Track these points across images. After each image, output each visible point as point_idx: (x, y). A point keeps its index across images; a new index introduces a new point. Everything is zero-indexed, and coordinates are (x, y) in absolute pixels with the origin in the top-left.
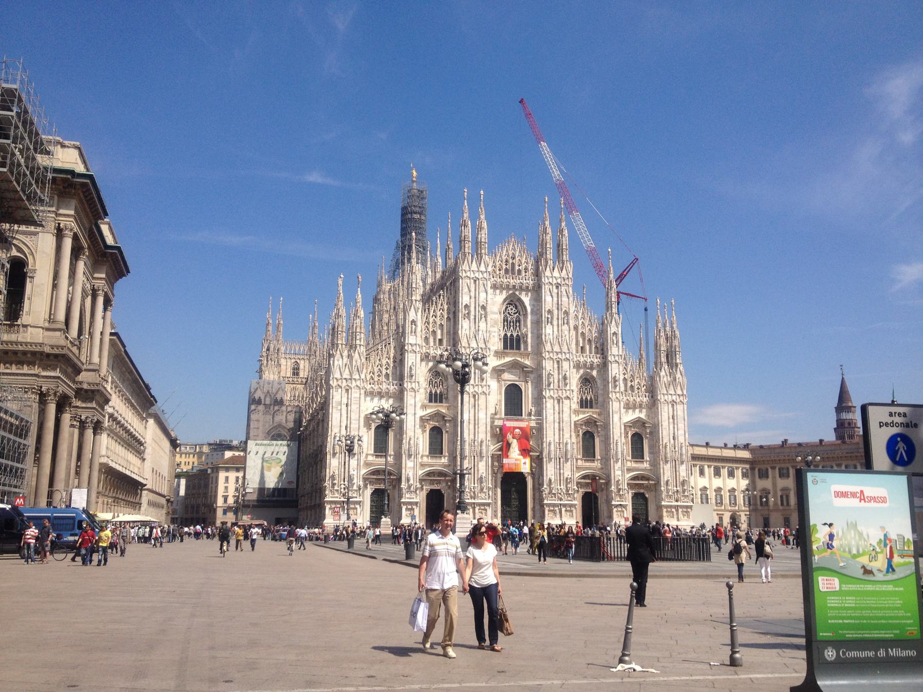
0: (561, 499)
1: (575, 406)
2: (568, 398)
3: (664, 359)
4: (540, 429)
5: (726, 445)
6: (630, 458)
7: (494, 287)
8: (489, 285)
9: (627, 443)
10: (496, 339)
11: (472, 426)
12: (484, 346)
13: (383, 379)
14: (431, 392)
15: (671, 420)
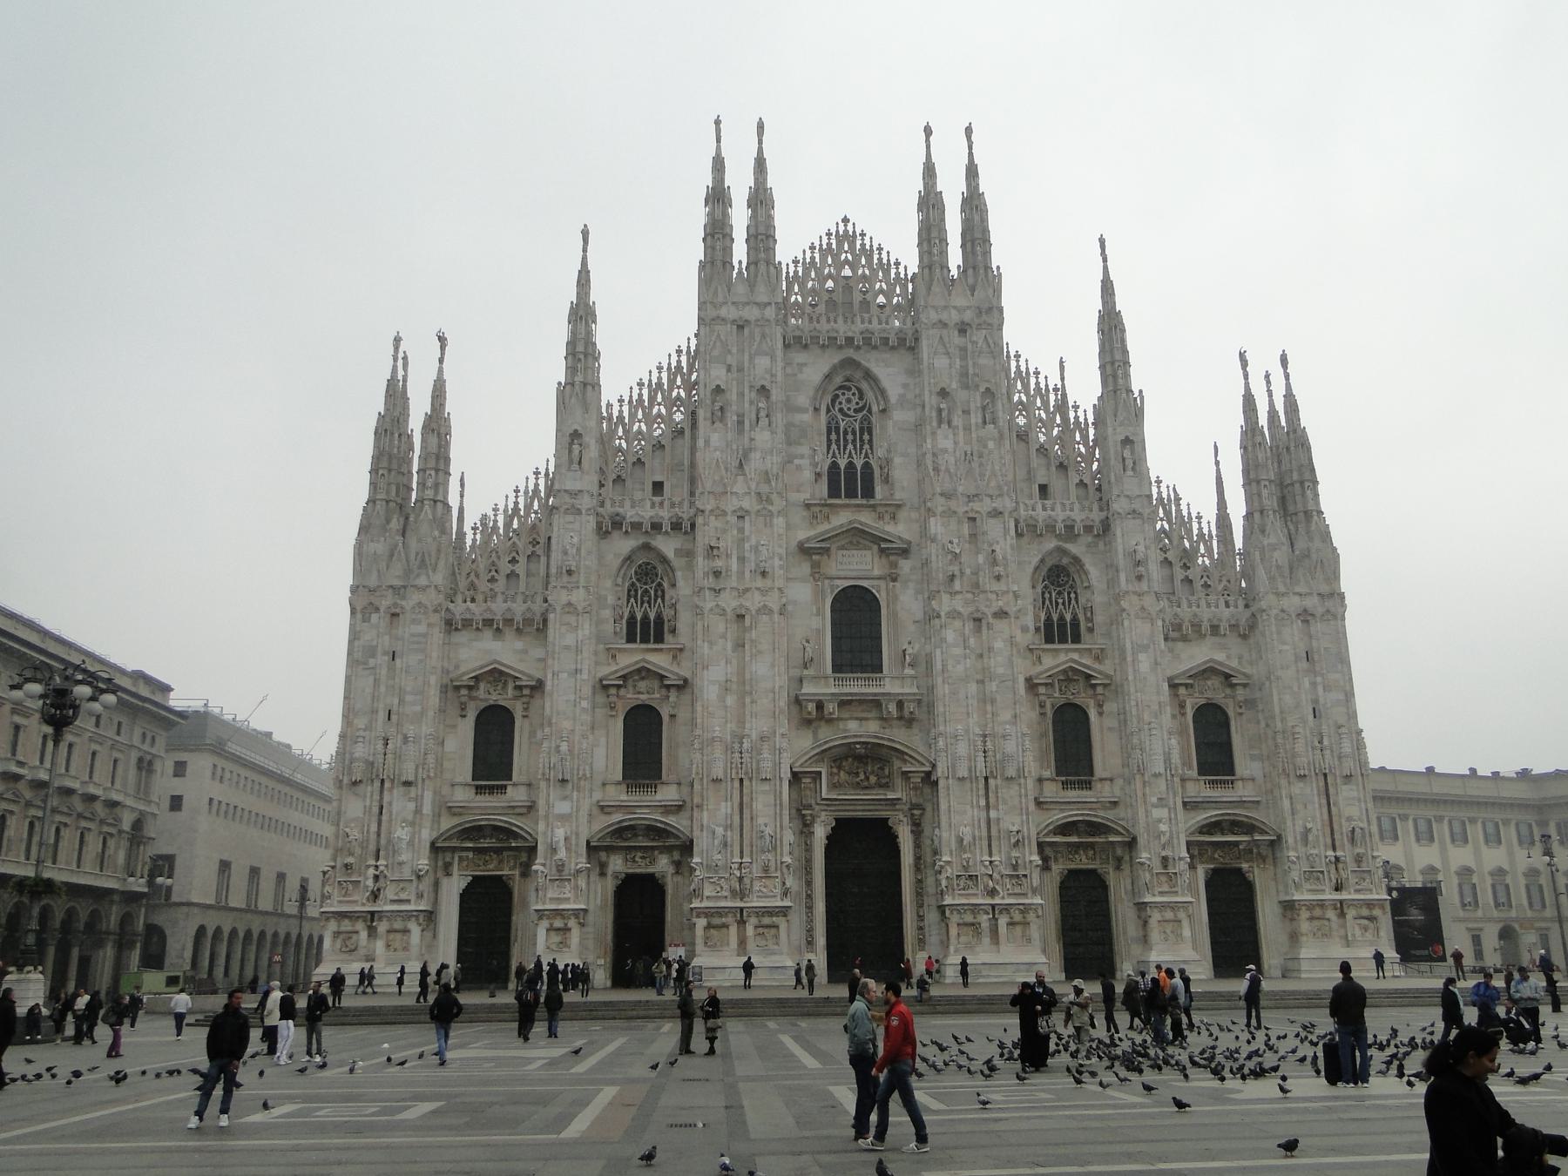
0: (992, 893)
1: (1028, 638)
2: (1002, 614)
3: (1271, 502)
4: (926, 702)
5: (1473, 771)
6: (1194, 773)
7: (794, 343)
8: (780, 344)
9: (1182, 732)
10: (808, 475)
11: (730, 700)
12: (764, 489)
13: (500, 585)
14: (632, 618)
15: (1304, 665)
